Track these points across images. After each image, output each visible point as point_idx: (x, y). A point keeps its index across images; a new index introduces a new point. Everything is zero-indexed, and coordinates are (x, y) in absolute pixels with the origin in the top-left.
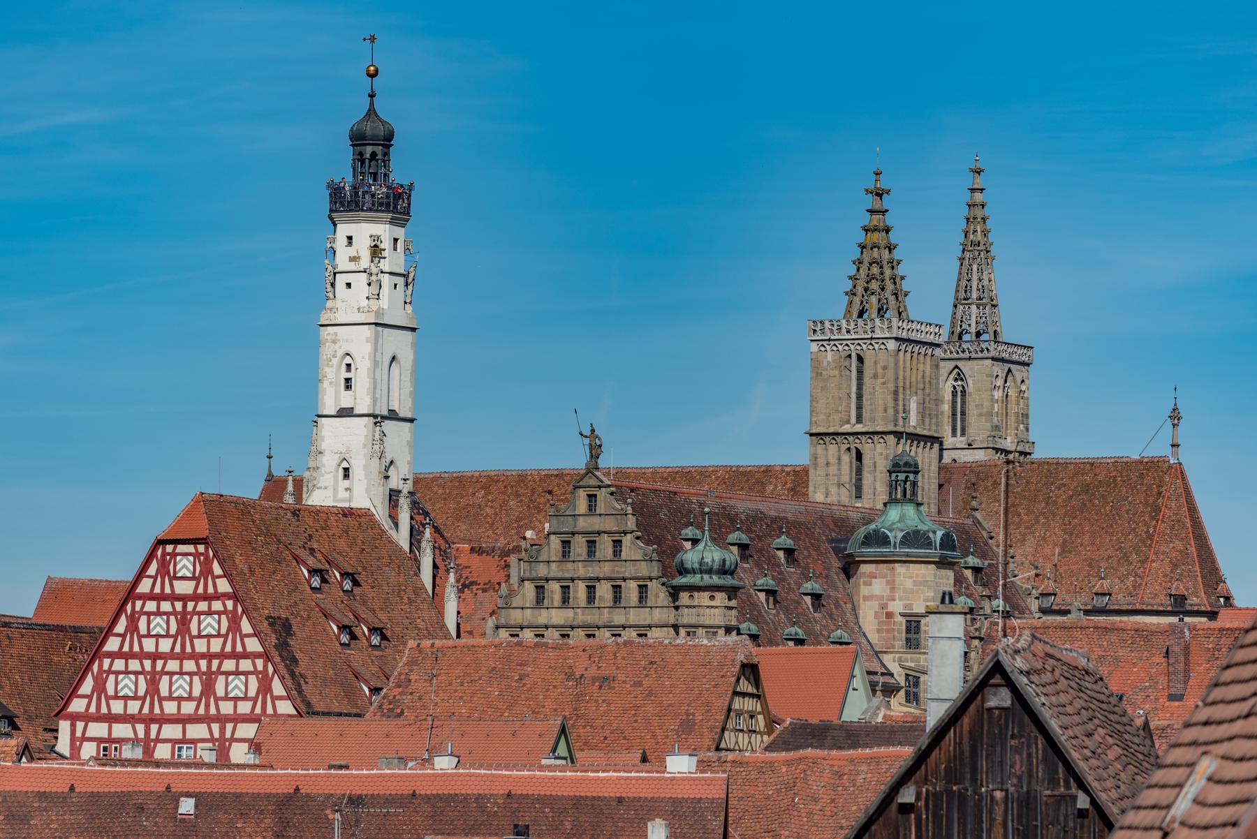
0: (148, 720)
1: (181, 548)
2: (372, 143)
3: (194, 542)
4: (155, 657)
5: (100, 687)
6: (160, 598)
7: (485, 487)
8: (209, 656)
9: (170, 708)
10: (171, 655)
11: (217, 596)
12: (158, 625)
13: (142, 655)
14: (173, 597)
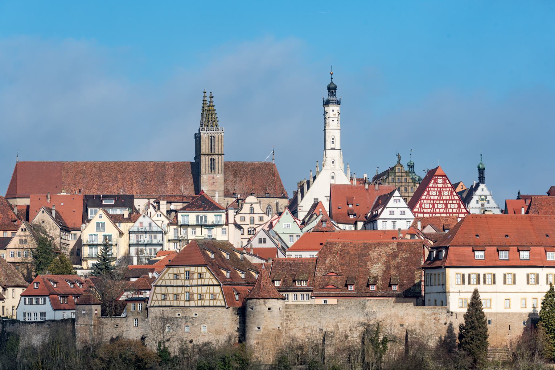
0: (432, 213)
1: (439, 177)
2: (332, 89)
3: (442, 176)
4: (433, 200)
5: (421, 206)
6: (434, 188)
7: (85, 165)
8: (446, 200)
9: (438, 211)
10: (437, 200)
11: (448, 187)
12: (434, 193)
13: (431, 200)
14: (438, 188)
